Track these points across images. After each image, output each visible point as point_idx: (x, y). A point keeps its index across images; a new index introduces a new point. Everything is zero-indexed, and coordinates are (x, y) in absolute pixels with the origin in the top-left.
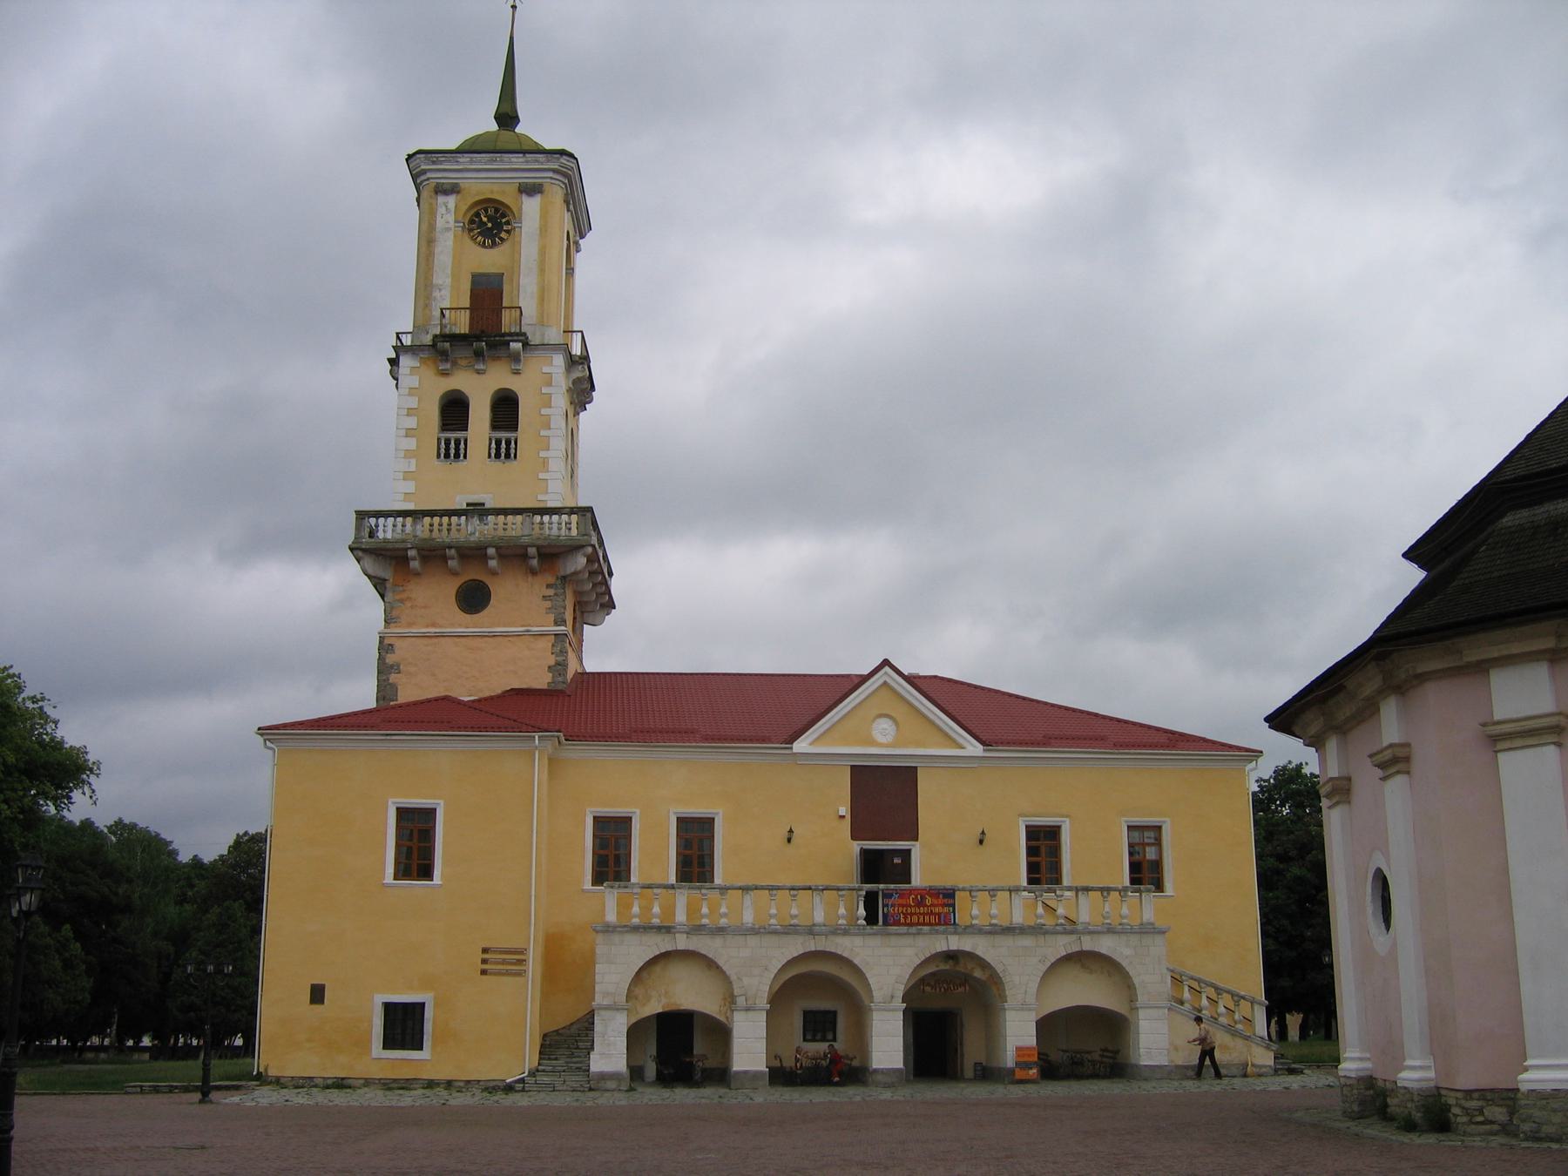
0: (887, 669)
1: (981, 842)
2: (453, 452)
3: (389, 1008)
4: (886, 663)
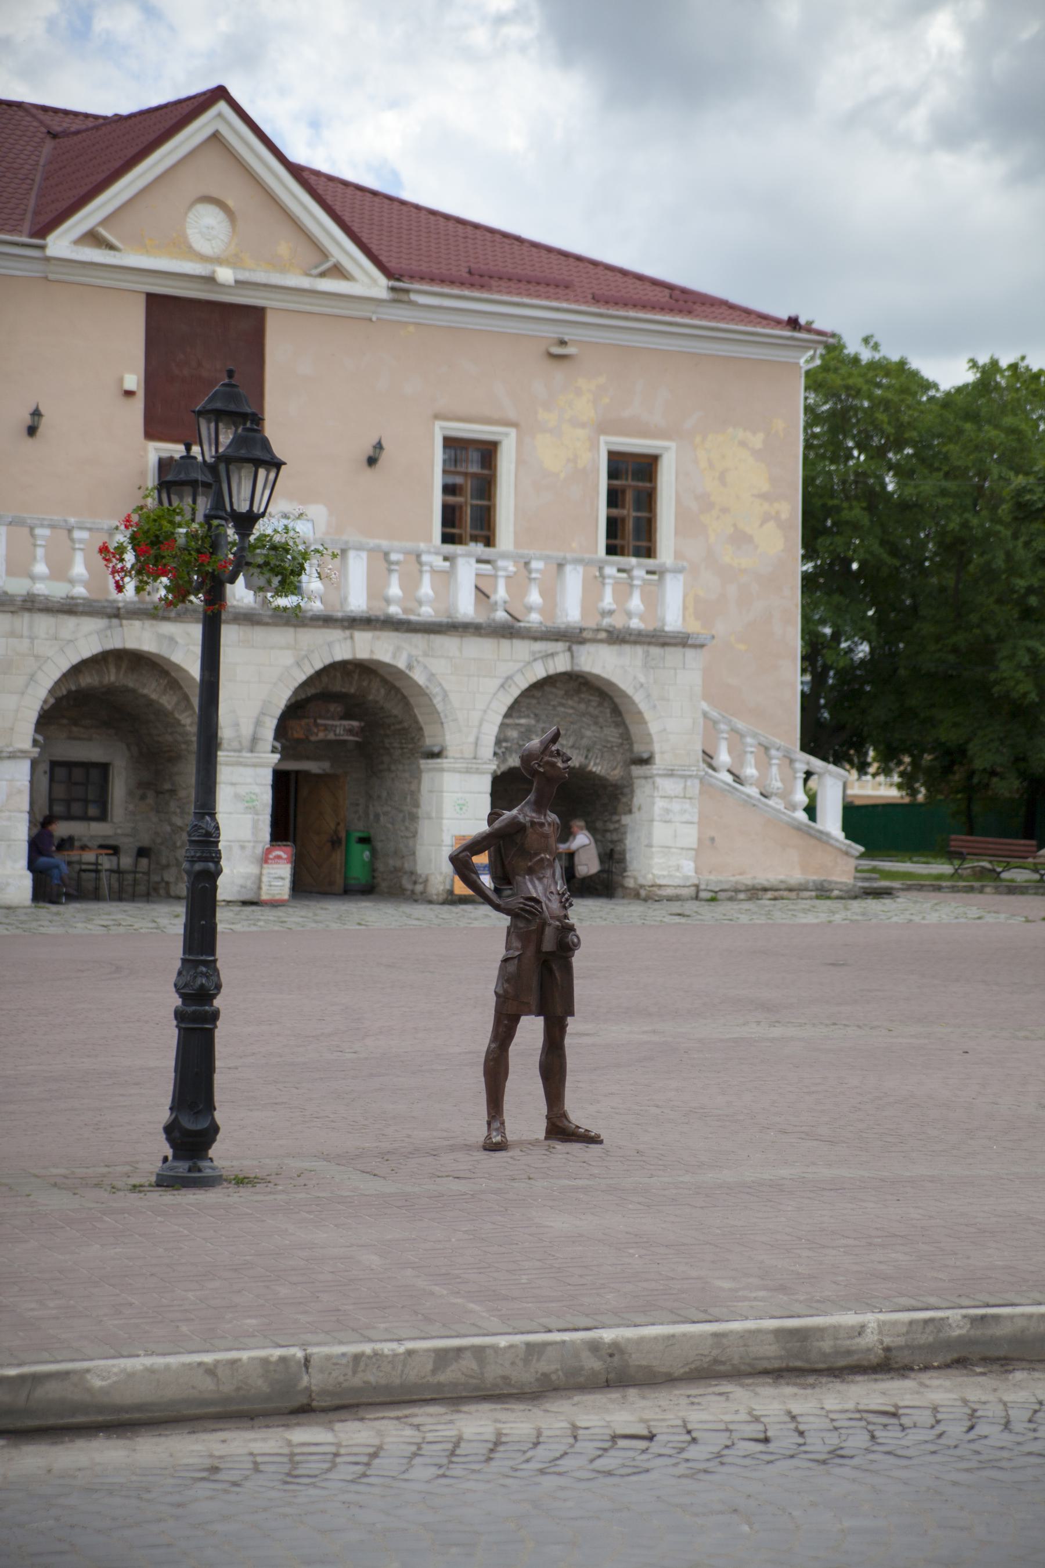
0: (222, 106)
1: (372, 461)
4: (220, 93)
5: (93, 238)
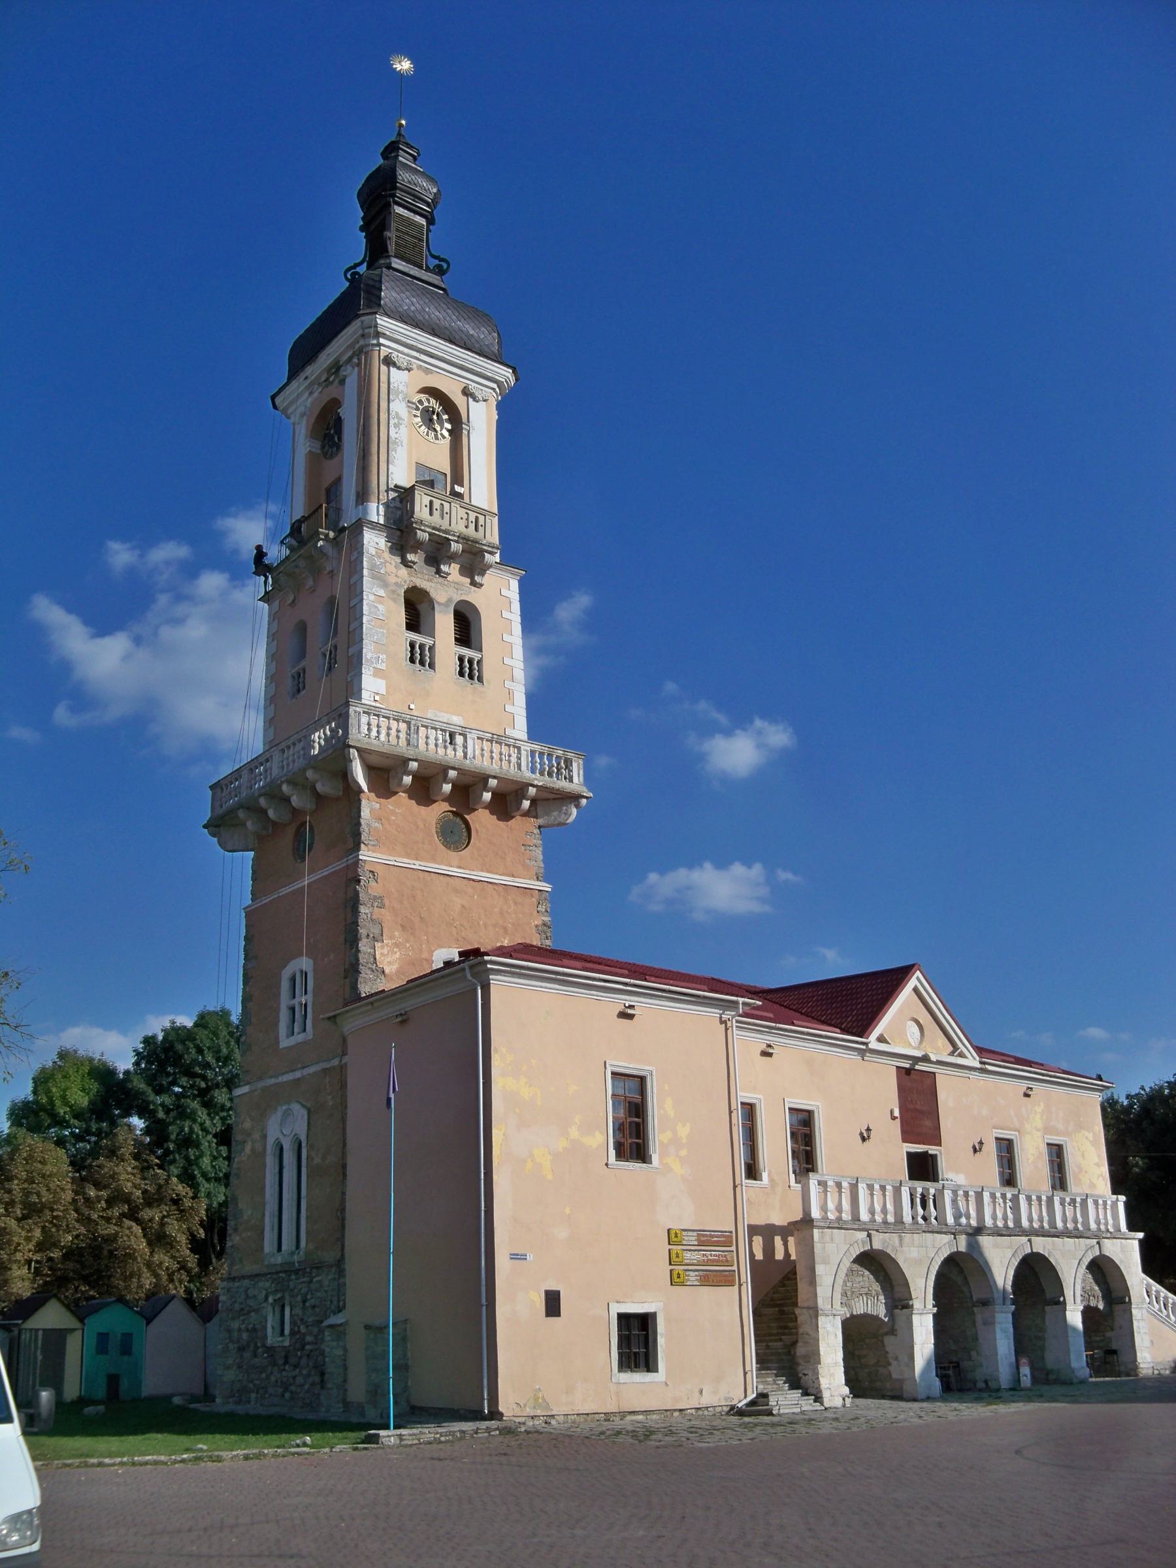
0: (918, 973)
2: (420, 657)
3: (623, 1318)
5: (881, 1039)
